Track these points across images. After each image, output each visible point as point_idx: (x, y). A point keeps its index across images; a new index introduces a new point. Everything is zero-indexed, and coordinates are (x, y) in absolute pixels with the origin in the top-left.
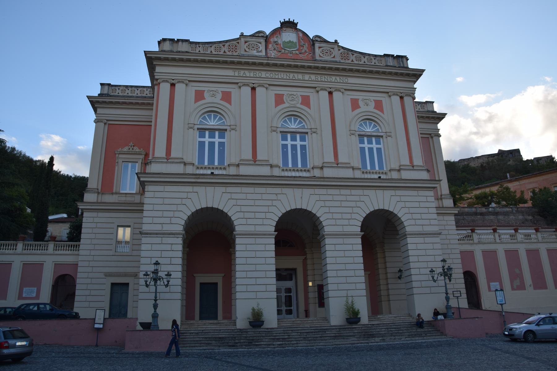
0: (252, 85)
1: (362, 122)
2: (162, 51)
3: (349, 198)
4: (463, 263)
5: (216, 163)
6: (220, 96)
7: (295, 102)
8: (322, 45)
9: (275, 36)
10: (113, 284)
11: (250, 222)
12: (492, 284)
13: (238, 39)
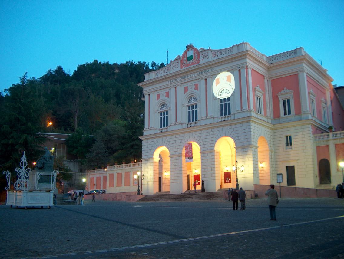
0: (175, 86)
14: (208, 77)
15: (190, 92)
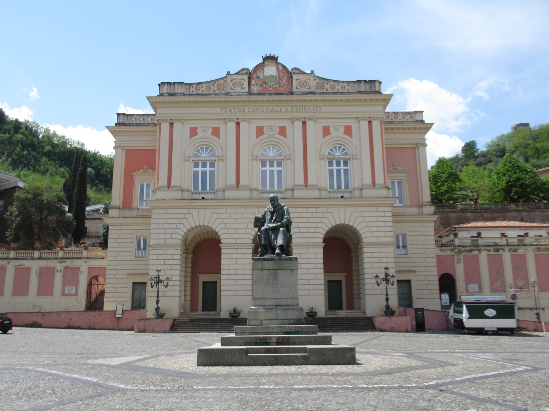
0: (237, 121)
1: (332, 147)
2: (161, 95)
3: (315, 215)
4: (438, 266)
5: (208, 189)
6: (210, 131)
7: (273, 133)
8: (300, 76)
9: (258, 72)
10: (134, 283)
11: (232, 236)
12: (471, 286)
13: (225, 77)
14: (310, 119)
15: (267, 138)
